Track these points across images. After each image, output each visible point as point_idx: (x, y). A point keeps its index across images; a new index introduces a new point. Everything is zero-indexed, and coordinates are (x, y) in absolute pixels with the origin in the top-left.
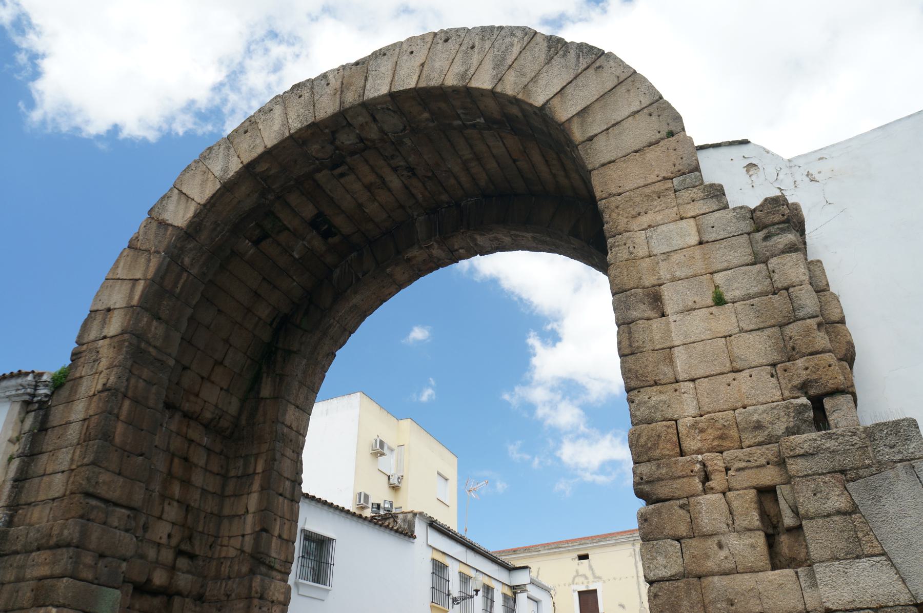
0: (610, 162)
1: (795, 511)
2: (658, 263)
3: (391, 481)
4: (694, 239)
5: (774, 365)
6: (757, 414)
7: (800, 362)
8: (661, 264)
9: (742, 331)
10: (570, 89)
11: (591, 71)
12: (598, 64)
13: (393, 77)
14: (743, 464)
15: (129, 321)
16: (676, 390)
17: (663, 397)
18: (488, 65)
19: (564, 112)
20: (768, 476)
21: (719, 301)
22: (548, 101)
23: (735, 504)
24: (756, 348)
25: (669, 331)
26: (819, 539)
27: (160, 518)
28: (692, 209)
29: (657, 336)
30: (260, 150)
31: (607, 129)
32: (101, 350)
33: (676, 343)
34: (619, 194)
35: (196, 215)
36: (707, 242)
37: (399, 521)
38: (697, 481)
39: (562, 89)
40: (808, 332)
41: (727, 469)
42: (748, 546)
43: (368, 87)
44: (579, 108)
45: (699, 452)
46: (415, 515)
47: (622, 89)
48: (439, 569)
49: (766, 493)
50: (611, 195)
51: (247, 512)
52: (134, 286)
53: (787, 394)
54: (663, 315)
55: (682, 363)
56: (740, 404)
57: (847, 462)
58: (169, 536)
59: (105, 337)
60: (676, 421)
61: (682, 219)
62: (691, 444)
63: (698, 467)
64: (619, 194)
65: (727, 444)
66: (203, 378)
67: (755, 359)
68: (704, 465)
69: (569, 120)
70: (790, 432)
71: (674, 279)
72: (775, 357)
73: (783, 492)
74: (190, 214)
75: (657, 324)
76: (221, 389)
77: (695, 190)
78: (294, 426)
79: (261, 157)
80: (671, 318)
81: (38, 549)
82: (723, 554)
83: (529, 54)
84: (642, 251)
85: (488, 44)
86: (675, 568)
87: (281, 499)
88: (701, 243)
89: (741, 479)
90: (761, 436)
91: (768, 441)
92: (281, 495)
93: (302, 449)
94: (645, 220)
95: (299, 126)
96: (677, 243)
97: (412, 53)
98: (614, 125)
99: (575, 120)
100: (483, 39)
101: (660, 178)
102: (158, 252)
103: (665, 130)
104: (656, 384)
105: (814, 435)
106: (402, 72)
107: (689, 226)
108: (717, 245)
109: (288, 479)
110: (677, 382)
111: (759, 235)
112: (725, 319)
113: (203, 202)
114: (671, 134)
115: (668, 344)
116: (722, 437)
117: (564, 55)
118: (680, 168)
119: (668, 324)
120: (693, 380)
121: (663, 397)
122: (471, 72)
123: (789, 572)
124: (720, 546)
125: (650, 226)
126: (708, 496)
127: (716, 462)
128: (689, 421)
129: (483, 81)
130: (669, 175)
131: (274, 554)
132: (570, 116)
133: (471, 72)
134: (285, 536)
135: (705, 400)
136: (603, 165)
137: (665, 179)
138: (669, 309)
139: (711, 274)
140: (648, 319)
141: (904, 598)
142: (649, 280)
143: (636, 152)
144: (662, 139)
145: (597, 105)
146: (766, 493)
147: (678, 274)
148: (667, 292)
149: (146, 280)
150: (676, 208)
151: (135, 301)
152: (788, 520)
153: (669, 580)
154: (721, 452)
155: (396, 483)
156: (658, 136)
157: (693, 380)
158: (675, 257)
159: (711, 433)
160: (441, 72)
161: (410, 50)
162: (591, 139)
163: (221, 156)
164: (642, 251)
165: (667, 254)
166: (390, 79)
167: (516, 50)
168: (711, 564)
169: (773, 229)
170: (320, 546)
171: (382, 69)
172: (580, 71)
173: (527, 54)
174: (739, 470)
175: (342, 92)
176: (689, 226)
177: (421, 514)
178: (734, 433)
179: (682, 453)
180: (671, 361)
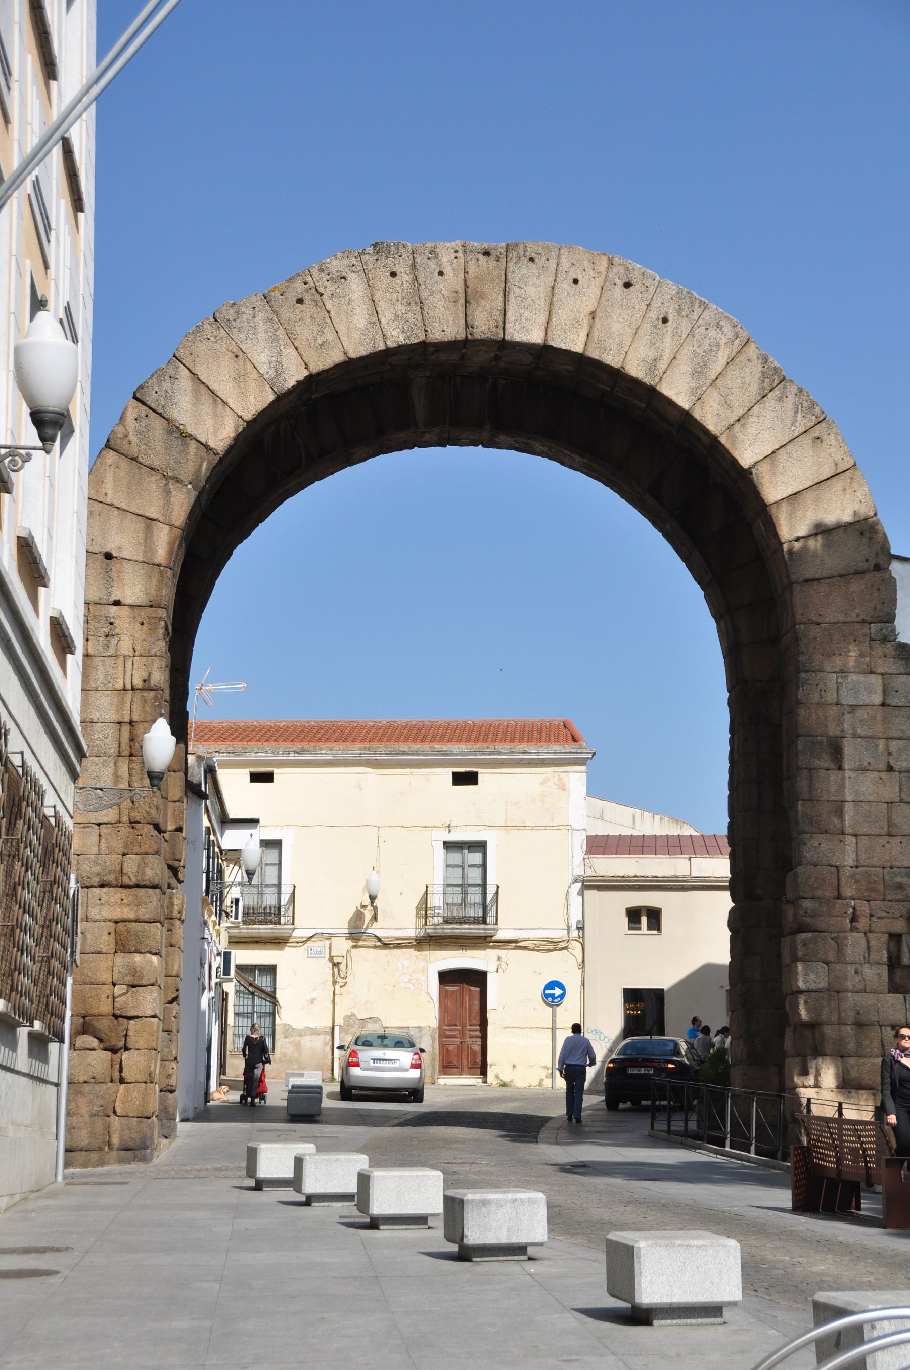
2: (843, 714)
4: (877, 699)
8: (847, 716)
9: (901, 801)
10: (782, 456)
11: (807, 440)
14: (884, 914)
15: (159, 589)
18: (684, 366)
19: (773, 490)
21: (890, 769)
22: (756, 463)
23: (872, 943)
25: (842, 786)
29: (833, 789)
30: (335, 357)
32: (117, 622)
33: (848, 799)
34: (818, 624)
36: (889, 705)
39: (773, 452)
41: (871, 915)
44: (790, 491)
49: (895, 938)
52: (148, 530)
56: (888, 865)
59: (117, 603)
61: (871, 672)
62: (848, 892)
64: (818, 624)
65: (873, 895)
68: (854, 909)
71: (855, 736)
75: (834, 776)
80: (848, 774)
81: (102, 886)
83: (737, 372)
84: (831, 697)
85: (685, 328)
86: (822, 984)
88: (883, 705)
89: (880, 925)
95: (402, 340)
96: (864, 698)
99: (784, 505)
100: (679, 311)
101: (860, 619)
104: (826, 832)
106: (562, 316)
107: (876, 681)
114: (877, 568)
115: (840, 798)
117: (780, 399)
118: (880, 614)
119: (843, 778)
122: (662, 365)
123: (900, 996)
124: (856, 972)
126: (855, 934)
127: (864, 908)
128: (848, 872)
130: (868, 618)
132: (779, 497)
133: (662, 365)
135: (863, 856)
136: (806, 581)
139: (887, 739)
140: (828, 770)
142: (833, 730)
143: (841, 576)
144: (869, 571)
145: (809, 496)
146: (895, 938)
147: (859, 731)
150: (868, 659)
154: (868, 901)
156: (865, 566)
157: (856, 835)
158: (861, 713)
160: (620, 344)
161: (573, 275)
163: (261, 335)
165: (853, 708)
166: (543, 318)
167: (722, 357)
171: (531, 290)
172: (796, 434)
173: (734, 372)
174: (879, 918)
176: (876, 681)
180: (839, 812)
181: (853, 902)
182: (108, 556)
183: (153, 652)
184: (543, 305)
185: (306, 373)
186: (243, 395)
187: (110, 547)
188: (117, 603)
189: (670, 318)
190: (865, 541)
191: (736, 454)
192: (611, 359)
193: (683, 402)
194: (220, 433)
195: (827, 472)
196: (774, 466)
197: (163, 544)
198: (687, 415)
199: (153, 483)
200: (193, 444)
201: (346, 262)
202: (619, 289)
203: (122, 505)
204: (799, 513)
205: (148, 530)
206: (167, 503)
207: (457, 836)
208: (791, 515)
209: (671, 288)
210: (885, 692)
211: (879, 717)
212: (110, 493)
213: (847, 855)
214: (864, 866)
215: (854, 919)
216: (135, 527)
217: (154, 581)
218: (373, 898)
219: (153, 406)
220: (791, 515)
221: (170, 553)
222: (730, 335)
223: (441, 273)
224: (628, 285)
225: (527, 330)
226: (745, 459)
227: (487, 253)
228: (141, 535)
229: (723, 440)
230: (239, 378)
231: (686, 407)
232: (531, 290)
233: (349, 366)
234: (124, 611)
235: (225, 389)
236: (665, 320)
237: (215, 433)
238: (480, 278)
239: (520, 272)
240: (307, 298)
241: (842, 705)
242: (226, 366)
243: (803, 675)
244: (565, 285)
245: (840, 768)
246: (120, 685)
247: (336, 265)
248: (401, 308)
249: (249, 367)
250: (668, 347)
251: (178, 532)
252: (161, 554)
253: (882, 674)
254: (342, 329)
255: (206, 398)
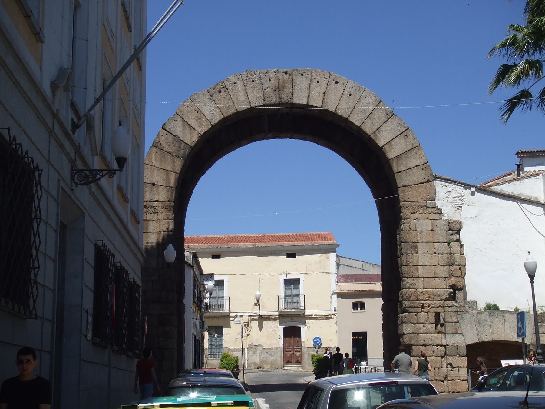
1: (444, 319)
4: (430, 229)
5: (446, 278)
6: (439, 291)
7: (453, 278)
15: (172, 195)
17: (414, 282)
19: (391, 154)
20: (440, 310)
21: (435, 253)
23: (429, 316)
24: (443, 271)
26: (449, 327)
28: (431, 216)
30: (233, 111)
40: (456, 270)
42: (431, 327)
45: (422, 300)
47: (414, 152)
50: (405, 201)
52: (167, 175)
54: (417, 254)
55: (421, 271)
57: (459, 310)
59: (157, 201)
65: (430, 299)
67: (441, 275)
70: (447, 299)
72: (447, 275)
73: (442, 314)
82: (425, 328)
88: (432, 230)
90: (439, 298)
91: (441, 300)
94: (416, 215)
96: (425, 228)
103: (427, 178)
105: (453, 301)
106: (313, 94)
107: (429, 222)
108: (437, 233)
111: (450, 232)
112: (436, 260)
116: (429, 297)
119: (418, 257)
121: (414, 282)
124: (424, 326)
129: (356, 120)
135: (426, 285)
136: (404, 186)
138: (419, 252)
141: (464, 344)
142: (414, 240)
146: (437, 315)
152: (442, 321)
153: (411, 334)
156: (424, 181)
157: (423, 278)
158: (424, 233)
159: (426, 295)
162: (400, 172)
164: (413, 229)
167: (371, 107)
168: (421, 331)
169: (454, 232)
178: (432, 296)
179: (418, 300)
182: (154, 184)
183: (170, 218)
184: (307, 91)
185: (222, 117)
186: (200, 126)
187: (154, 181)
188: (157, 201)
189: (352, 94)
190: (424, 172)
191: (377, 142)
192: (332, 109)
193: (358, 124)
194: (191, 139)
195: (410, 147)
196: (391, 145)
197: (172, 181)
198: (359, 128)
199: (169, 158)
200: (183, 144)
201: (236, 77)
202: (334, 84)
203: (158, 166)
204: (400, 163)
205: (167, 175)
206: (174, 165)
207: (290, 277)
208: (398, 163)
209: (351, 83)
211: (430, 235)
212: (154, 162)
213: (420, 286)
216: (163, 174)
217: (170, 193)
218: (258, 301)
219: (169, 131)
220: (398, 163)
221: (175, 182)
222: (374, 99)
223: (270, 80)
224: (337, 83)
225: (301, 99)
226: (381, 144)
227: (286, 73)
228: (165, 176)
229: (372, 137)
230: (199, 119)
231: (359, 125)
232: (302, 86)
233: (238, 114)
234: (160, 204)
235: (194, 124)
236: (350, 95)
237: (191, 139)
238: (284, 82)
239: (298, 79)
240: (222, 91)
242: (195, 115)
244: (314, 84)
246: (158, 230)
247: (232, 78)
248: (256, 94)
249: (202, 116)
250: (352, 104)
251: (178, 175)
252: (172, 183)
254: (235, 101)
255: (187, 126)
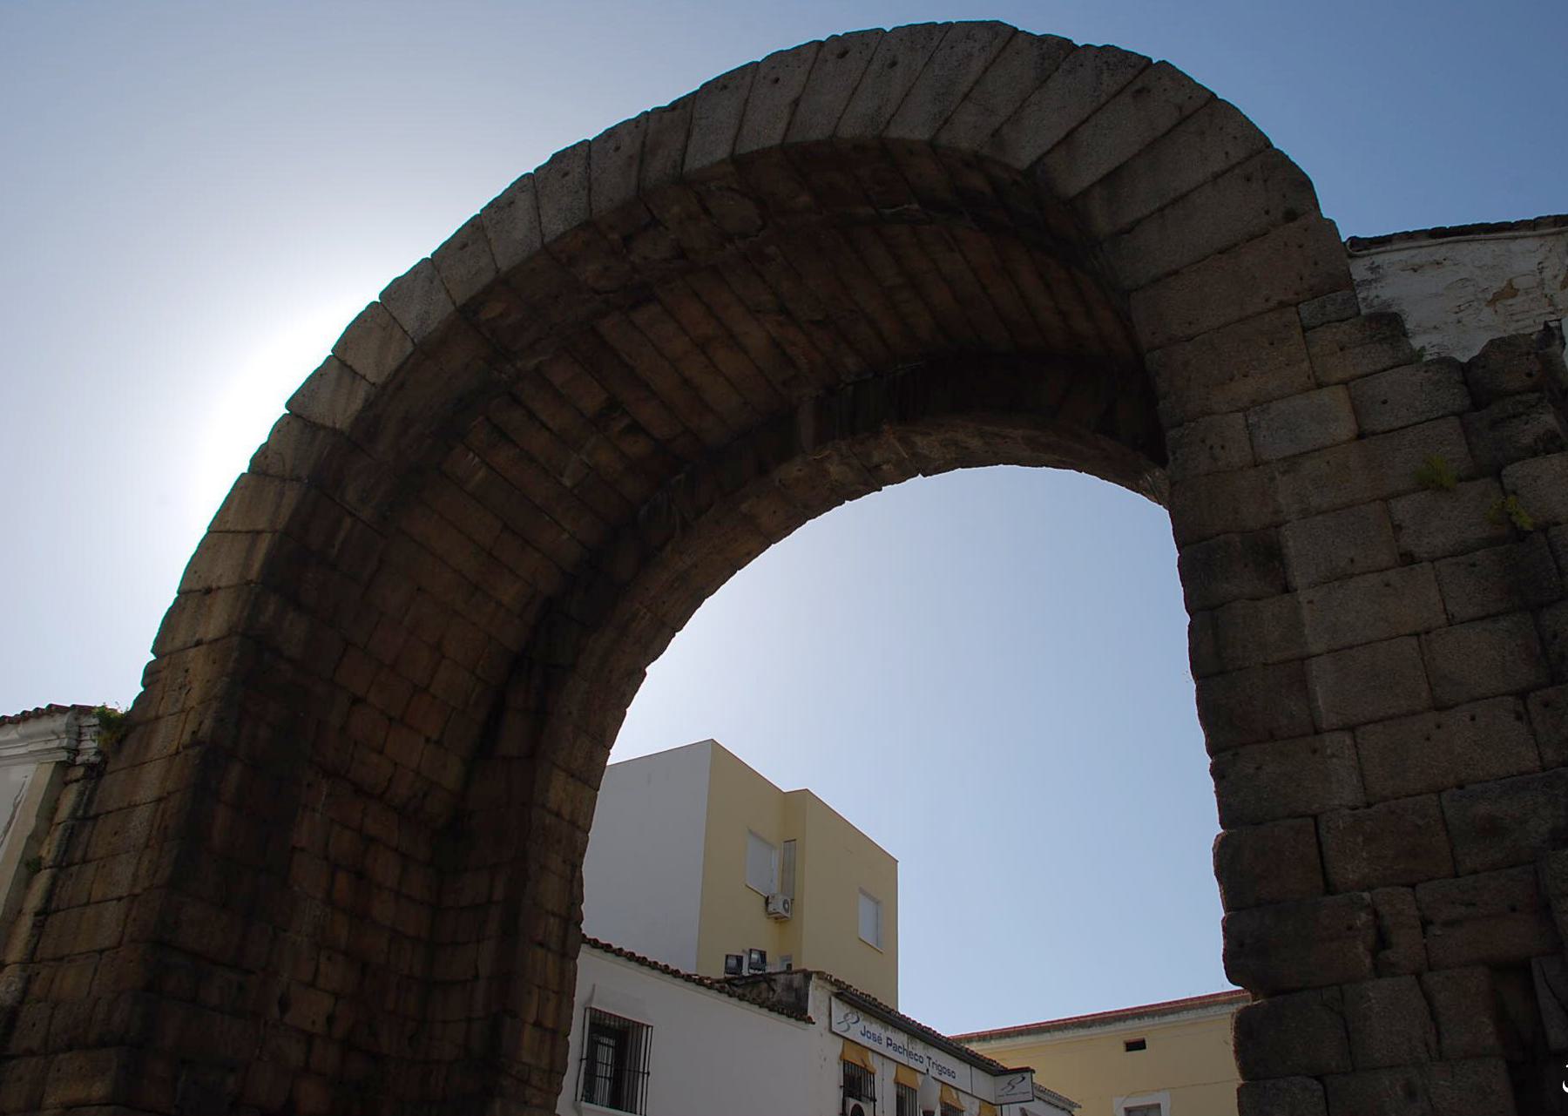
0: (1169, 275)
2: (1272, 479)
3: (771, 908)
4: (1344, 428)
5: (1522, 695)
9: (1450, 622)
12: (1139, 84)
13: (740, 128)
16: (1315, 751)
22: (1040, 159)
27: (312, 984)
31: (1161, 209)
33: (1314, 649)
34: (1190, 339)
35: (369, 404)
36: (1374, 434)
37: (778, 989)
38: (1361, 948)
39: (1068, 135)
43: (691, 150)
44: (1104, 170)
46: (807, 975)
48: (856, 1083)
51: (477, 977)
53: (1550, 755)
58: (330, 1019)
59: (198, 643)
60: (1315, 817)
61: (1320, 386)
63: (1363, 917)
64: (1190, 339)
66: (390, 719)
69: (1085, 193)
74: (357, 404)
76: (428, 740)
77: (1345, 326)
78: (566, 811)
79: (488, 292)
80: (1303, 596)
87: (540, 952)
88: (1361, 436)
92: (541, 945)
93: (582, 856)
97: (777, 80)
98: (1175, 201)
101: (1272, 303)
102: (298, 479)
109: (553, 914)
110: (1317, 732)
113: (380, 380)
114: (1291, 216)
120: (1351, 729)
124: (1411, 1094)
125: (1254, 402)
129: (914, 128)
131: (526, 1058)
134: (549, 1023)
137: (1282, 305)
138: (1298, 580)
139: (1385, 500)
140: (1255, 599)
148: (1294, 543)
149: (274, 532)
150: (1306, 365)
151: (254, 573)
154: (1413, 886)
155: (780, 909)
157: (1351, 729)
161: (773, 76)
165: (1291, 463)
167: (977, 66)
170: (621, 1042)
174: (1448, 924)
175: (642, 161)
176: (1334, 400)
177: (821, 975)
179: (1329, 889)
181: (1366, 895)
210: (1356, 411)
214: (1385, 799)
215: (1382, 941)
241: (1267, 463)
243: (1172, 433)
245: (1287, 589)
253: (1345, 383)
